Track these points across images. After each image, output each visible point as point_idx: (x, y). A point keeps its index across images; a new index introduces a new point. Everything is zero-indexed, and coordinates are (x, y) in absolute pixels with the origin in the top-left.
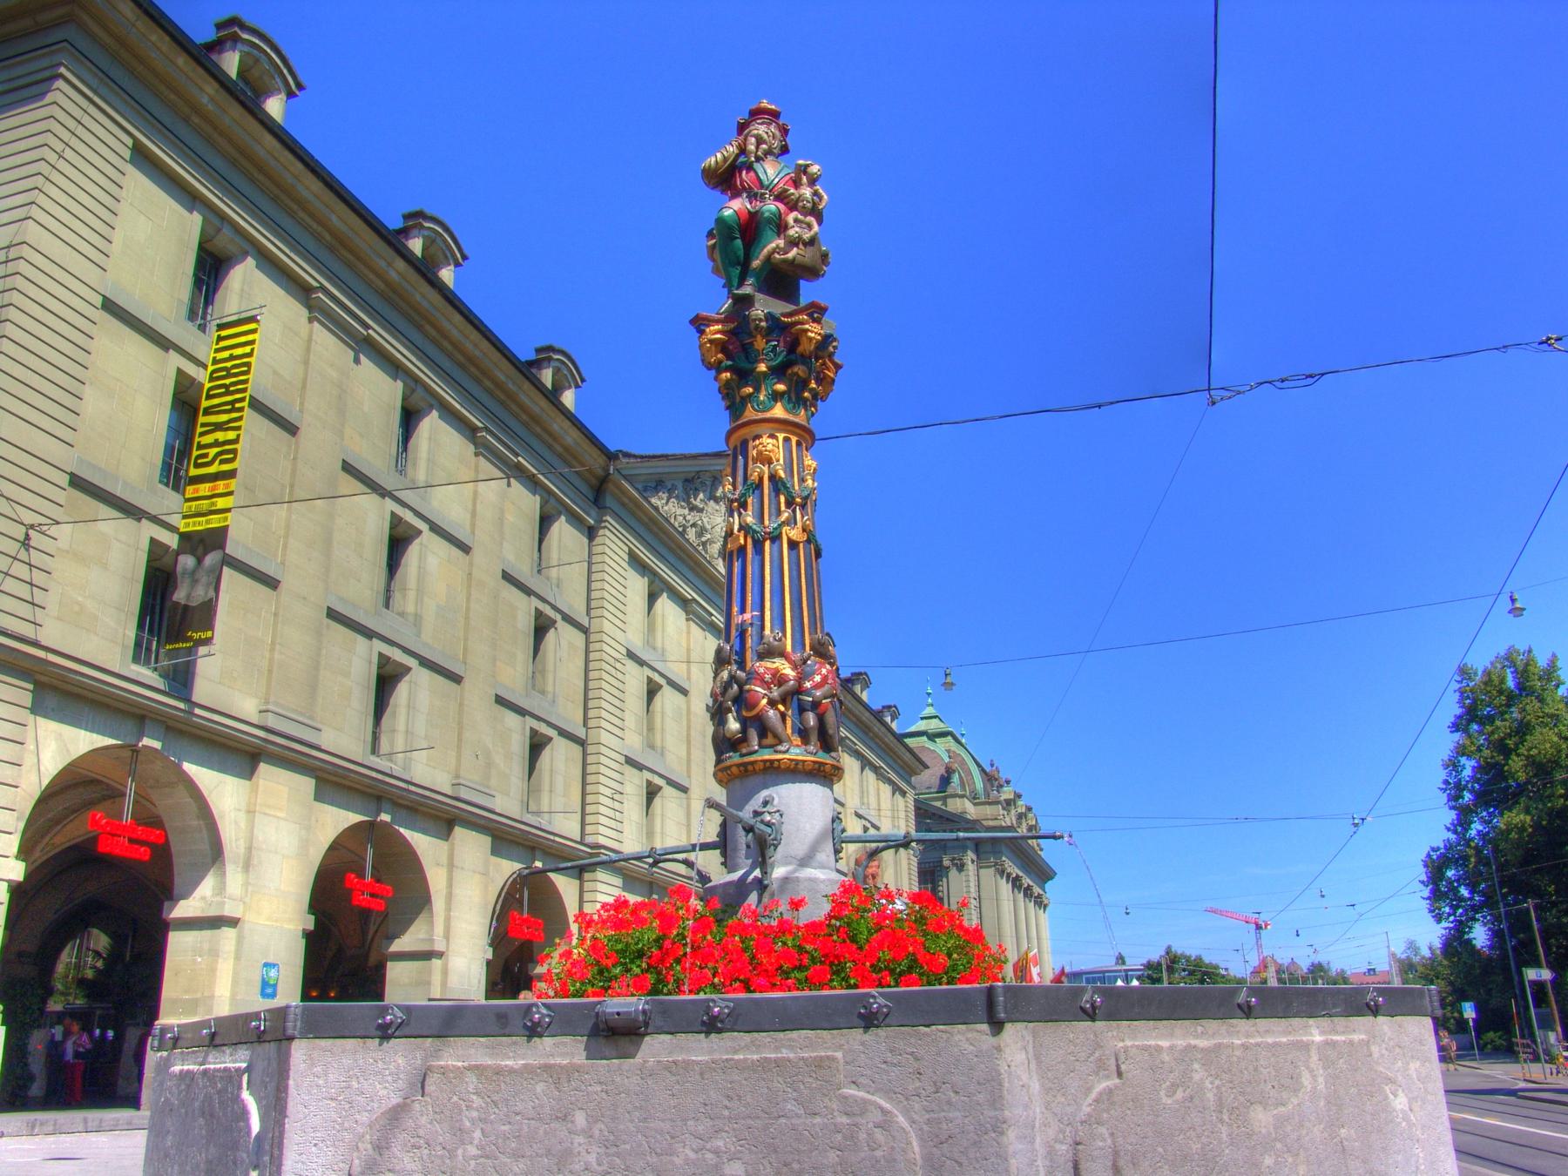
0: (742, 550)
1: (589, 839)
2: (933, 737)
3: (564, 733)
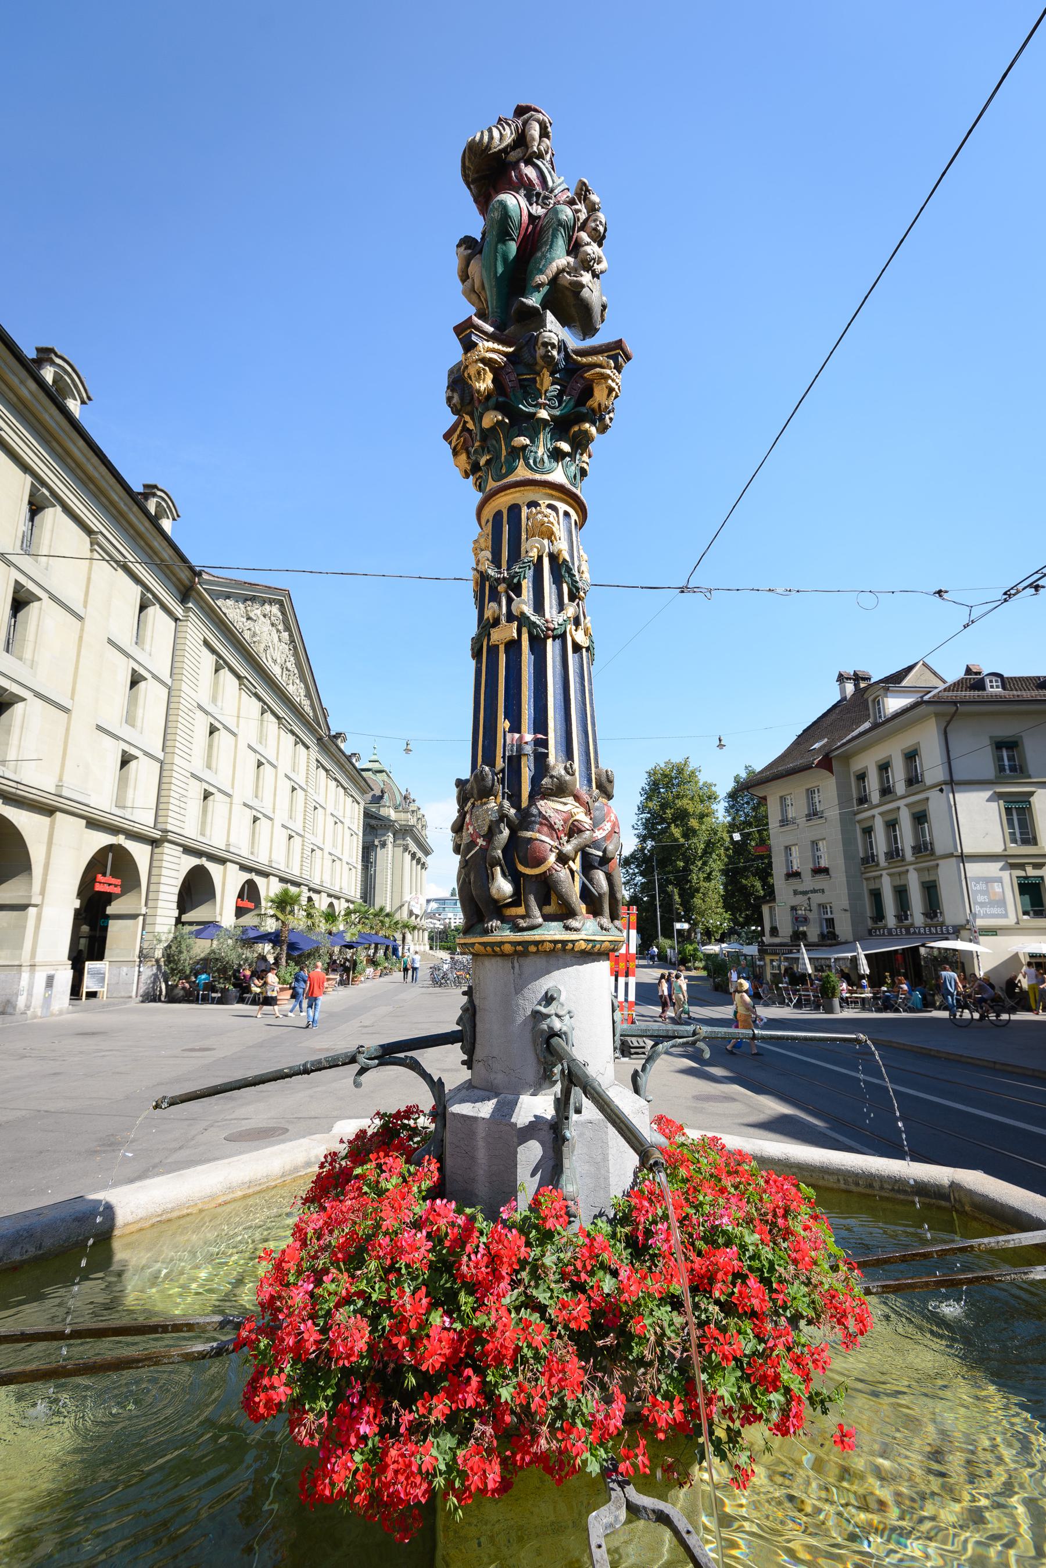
0: (513, 646)
1: (159, 826)
3: (146, 754)
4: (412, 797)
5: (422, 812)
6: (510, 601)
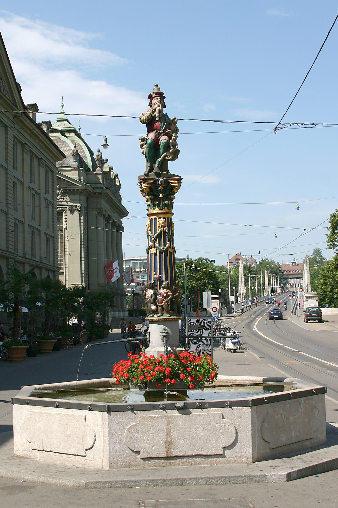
2: (63, 133)
4: (104, 158)
5: (114, 171)
6: (154, 243)
